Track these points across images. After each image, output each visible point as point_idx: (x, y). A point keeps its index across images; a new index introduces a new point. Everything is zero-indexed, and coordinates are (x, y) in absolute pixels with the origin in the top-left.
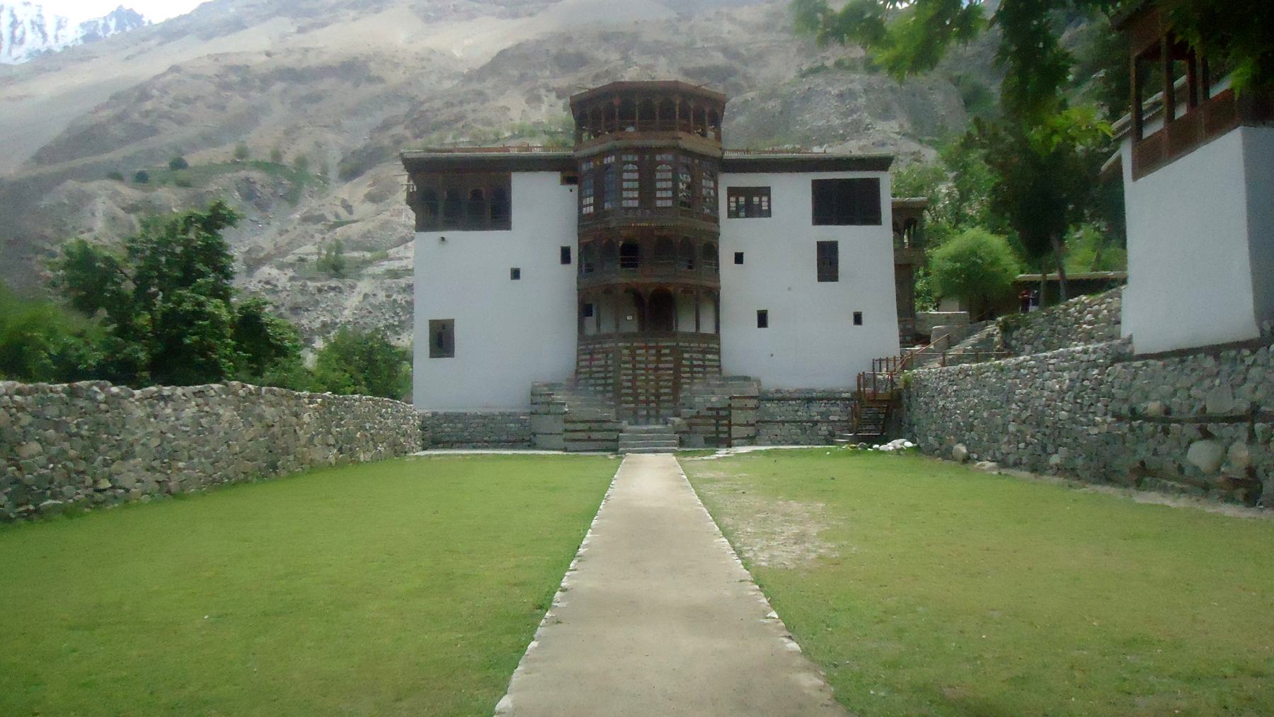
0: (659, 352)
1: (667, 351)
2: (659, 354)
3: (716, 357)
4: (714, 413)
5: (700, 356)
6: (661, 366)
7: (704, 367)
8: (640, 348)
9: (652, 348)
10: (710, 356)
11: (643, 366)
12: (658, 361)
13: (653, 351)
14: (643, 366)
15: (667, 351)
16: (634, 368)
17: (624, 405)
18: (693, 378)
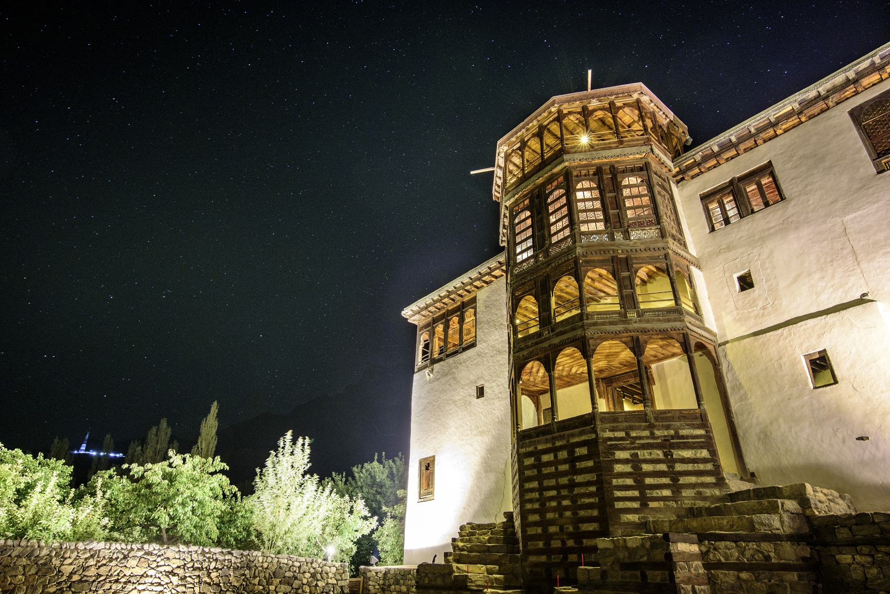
0: (571, 453)
1: (583, 451)
2: (573, 460)
3: (704, 453)
4: (638, 573)
5: (659, 454)
6: (579, 479)
7: (675, 476)
8: (546, 451)
9: (561, 448)
10: (687, 454)
11: (553, 482)
12: (575, 471)
13: (563, 455)
14: (553, 482)
15: (583, 451)
16: (541, 489)
17: (533, 559)
18: (644, 500)
